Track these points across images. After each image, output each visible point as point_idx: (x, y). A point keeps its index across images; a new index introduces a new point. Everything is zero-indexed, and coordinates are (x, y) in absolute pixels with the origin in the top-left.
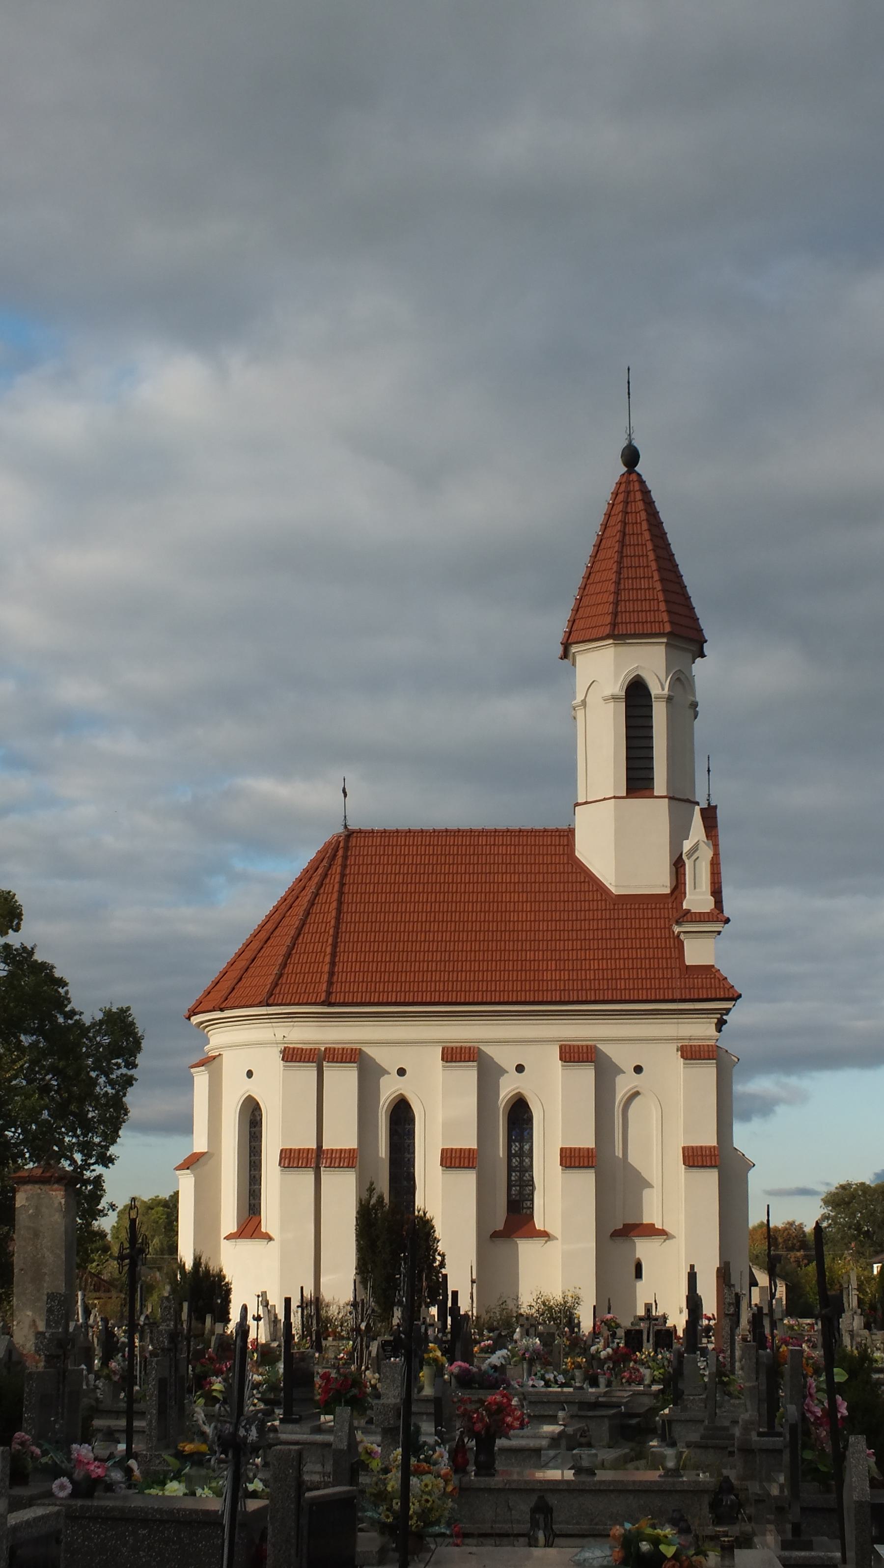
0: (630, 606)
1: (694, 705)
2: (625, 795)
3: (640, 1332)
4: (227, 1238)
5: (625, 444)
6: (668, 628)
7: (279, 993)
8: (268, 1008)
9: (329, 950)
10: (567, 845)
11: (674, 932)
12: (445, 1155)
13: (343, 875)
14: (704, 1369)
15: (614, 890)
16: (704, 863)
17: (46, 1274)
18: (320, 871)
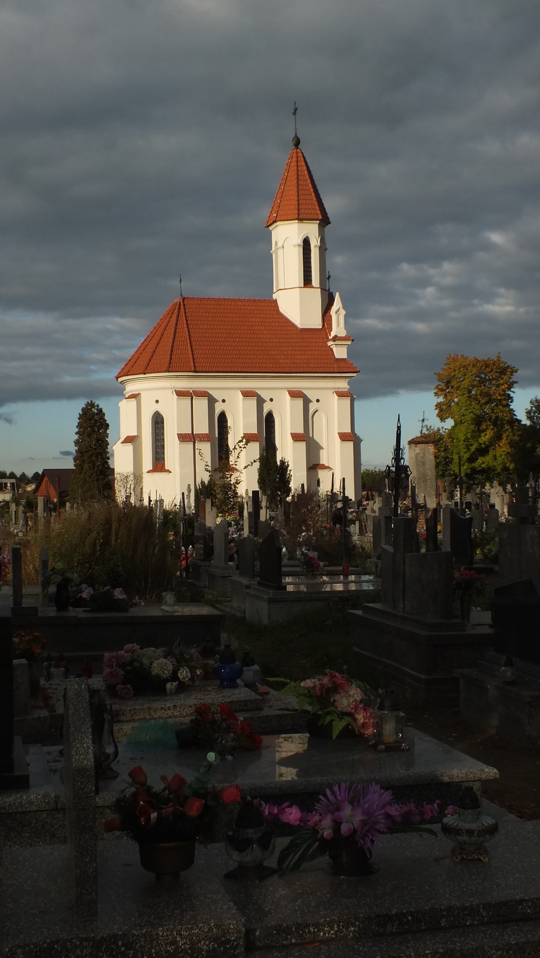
2: (303, 286)
4: (148, 472)
5: (294, 136)
15: (300, 326)
16: (342, 316)
17: (428, 479)
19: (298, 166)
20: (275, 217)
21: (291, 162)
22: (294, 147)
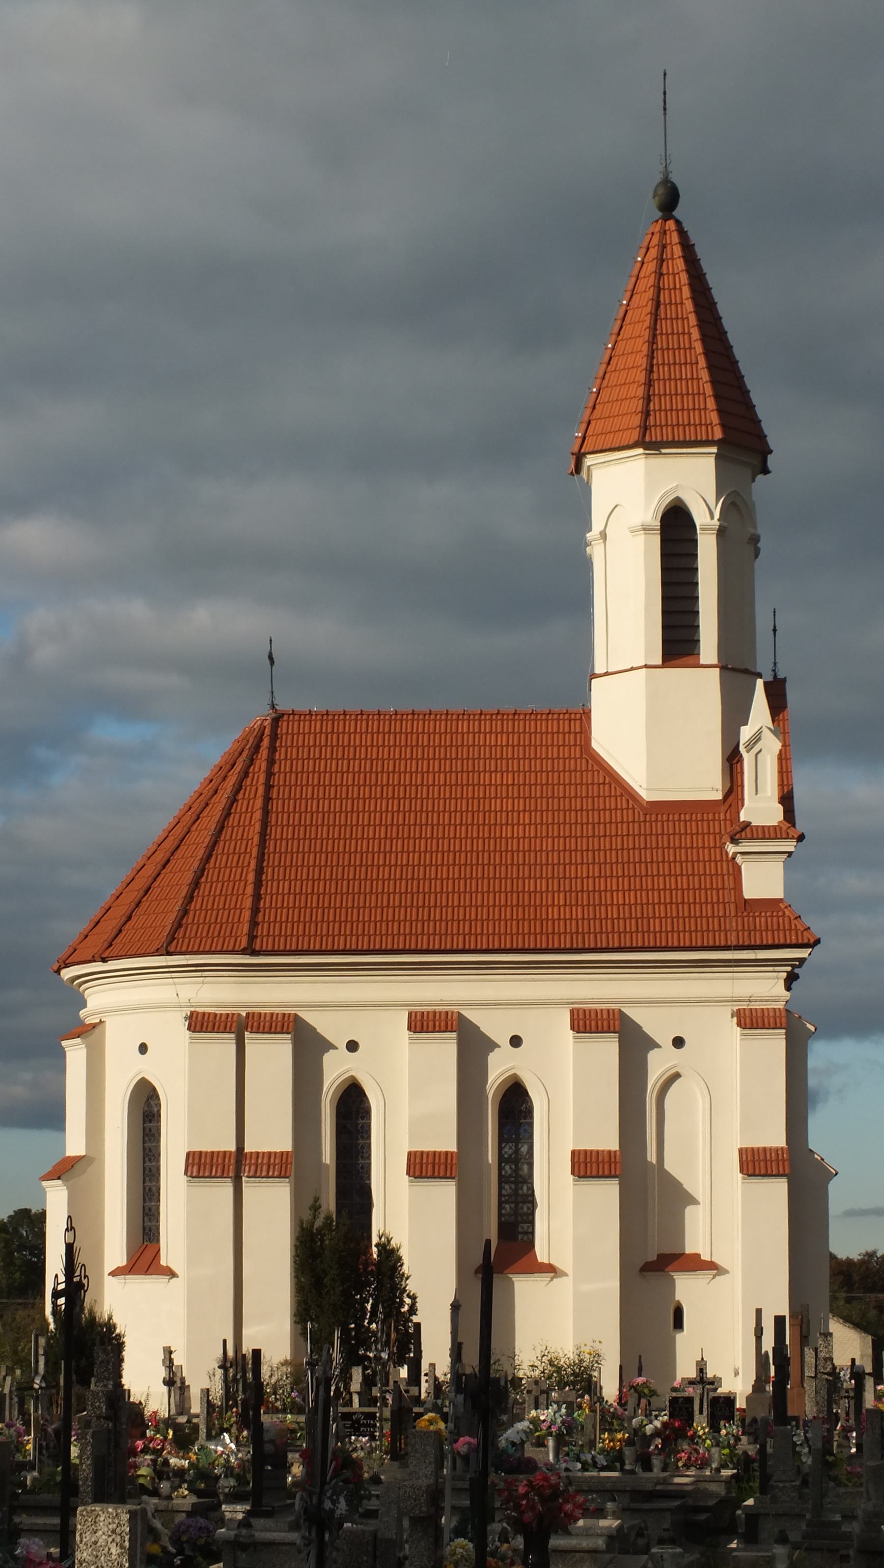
0: (666, 403)
1: (755, 540)
2: (659, 661)
3: (690, 1400)
4: (113, 1274)
5: (658, 178)
6: (718, 434)
7: (184, 937)
8: (168, 957)
9: (251, 877)
10: (581, 733)
11: (727, 854)
12: (744, 1159)
13: (270, 774)
14: (801, 1445)
15: (646, 795)
16: (769, 758)
18: (238, 767)
19: (661, 274)
20: (579, 441)
21: (643, 263)
22: (659, 214)
